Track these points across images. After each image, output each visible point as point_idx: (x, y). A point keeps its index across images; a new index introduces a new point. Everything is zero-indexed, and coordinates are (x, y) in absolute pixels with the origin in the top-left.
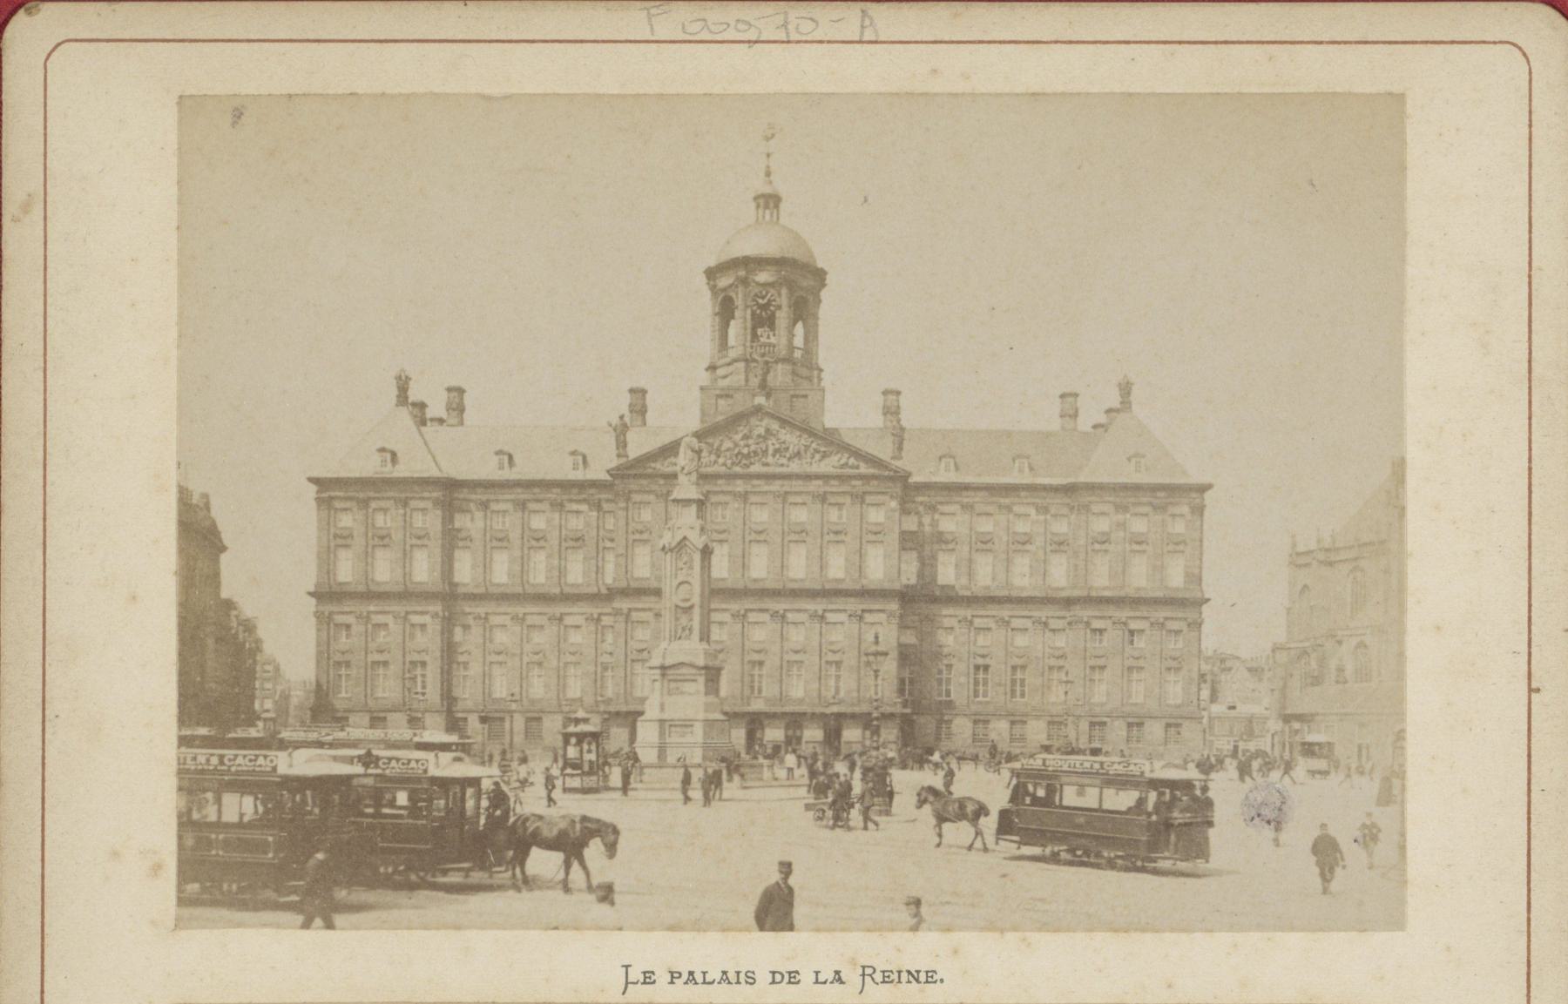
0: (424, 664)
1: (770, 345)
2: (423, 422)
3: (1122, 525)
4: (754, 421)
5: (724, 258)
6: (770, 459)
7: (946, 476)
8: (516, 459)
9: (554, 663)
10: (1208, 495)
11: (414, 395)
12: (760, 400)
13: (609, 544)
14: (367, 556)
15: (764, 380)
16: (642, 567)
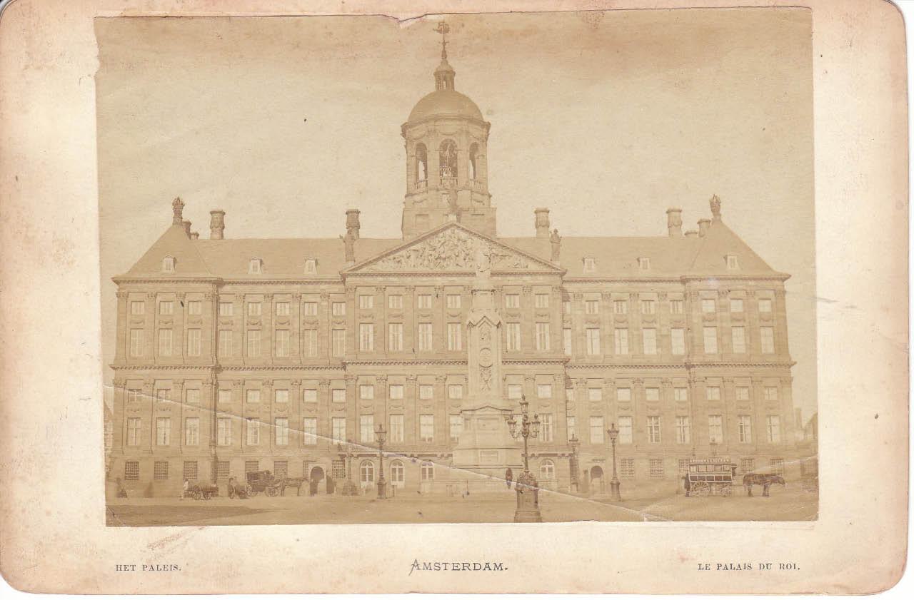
3: (725, 308)
4: (448, 232)
8: (264, 261)
11: (186, 216)
12: (453, 218)
13: (338, 327)
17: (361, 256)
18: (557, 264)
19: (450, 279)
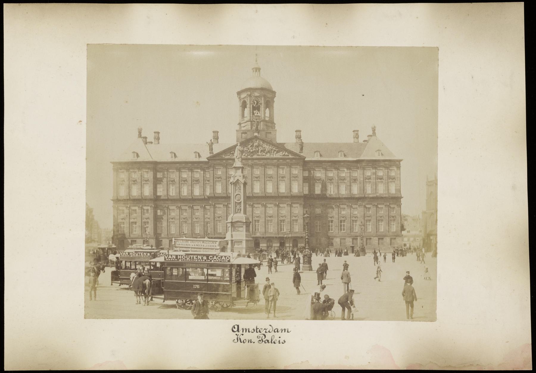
0: (148, 222)
1: (258, 116)
2: (146, 143)
3: (375, 174)
4: (254, 140)
6: (260, 153)
7: (317, 158)
9: (190, 221)
10: (401, 163)
11: (143, 135)
13: (207, 182)
14: (129, 188)
15: (257, 127)
16: (219, 189)
17: (216, 150)
18: (302, 154)
19: (255, 161)
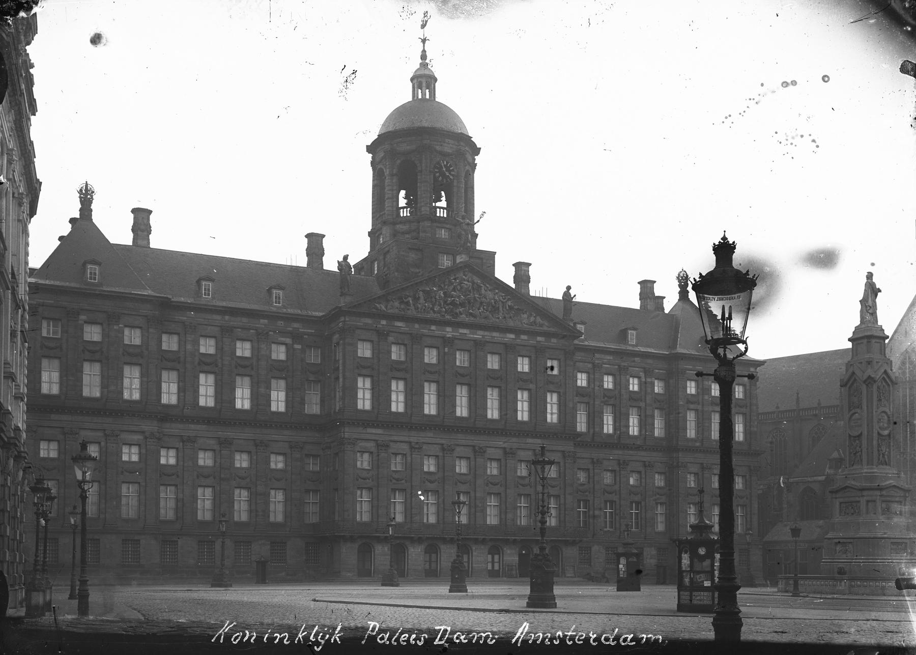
5: (399, 126)
